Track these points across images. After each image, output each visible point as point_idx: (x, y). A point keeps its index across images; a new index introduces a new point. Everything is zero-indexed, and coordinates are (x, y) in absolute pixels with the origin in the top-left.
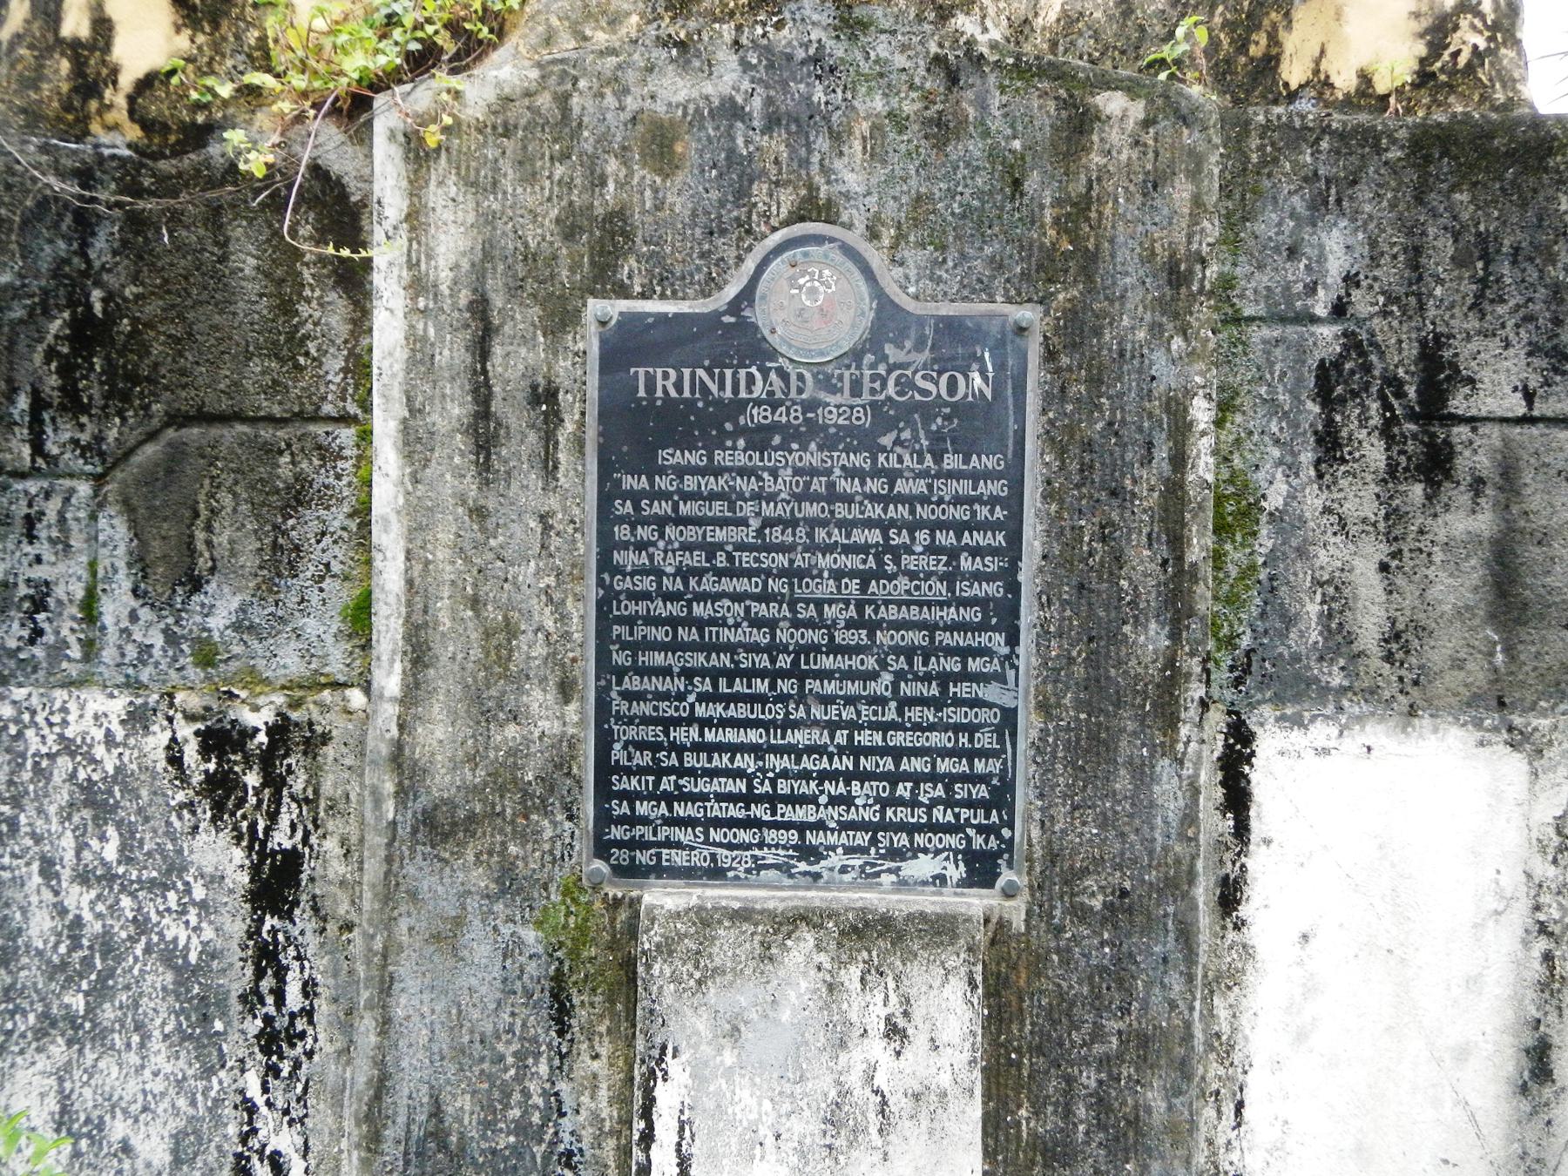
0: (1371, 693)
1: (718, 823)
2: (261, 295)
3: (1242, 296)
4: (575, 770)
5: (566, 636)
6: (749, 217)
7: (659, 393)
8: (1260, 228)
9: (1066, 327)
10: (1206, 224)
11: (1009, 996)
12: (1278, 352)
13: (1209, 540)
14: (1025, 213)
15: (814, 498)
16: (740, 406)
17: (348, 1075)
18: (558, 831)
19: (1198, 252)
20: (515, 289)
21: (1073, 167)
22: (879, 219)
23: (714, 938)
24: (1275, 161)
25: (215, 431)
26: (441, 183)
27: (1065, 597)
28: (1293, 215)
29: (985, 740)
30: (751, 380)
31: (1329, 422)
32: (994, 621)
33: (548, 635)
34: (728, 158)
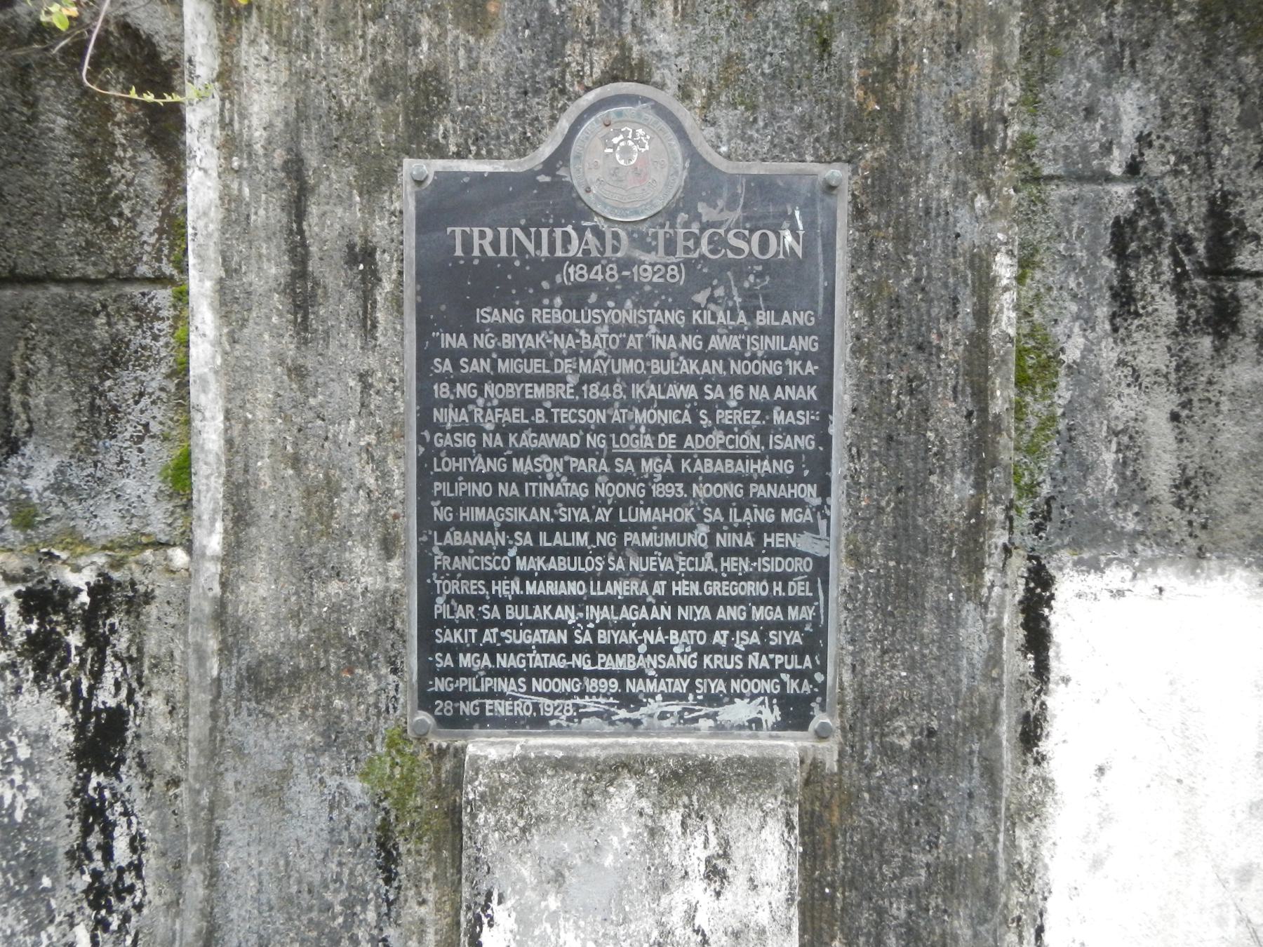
0: (1163, 537)
1: (540, 673)
2: (72, 156)
3: (1041, 156)
4: (398, 625)
5: (388, 493)
6: (563, 77)
7: (476, 253)
8: (1058, 89)
9: (873, 186)
10: (1007, 84)
11: (823, 833)
12: (1076, 210)
13: (1012, 393)
14: (833, 73)
16: (556, 265)
17: (177, 926)
18: (383, 685)
19: (1000, 112)
20: (329, 149)
21: (879, 29)
22: (691, 79)
23: (537, 787)
24: (1073, 23)
25: (29, 293)
26: (253, 42)
27: (875, 448)
28: (1090, 76)
29: (798, 588)
30: (567, 238)
31: (1124, 278)
32: (806, 473)
33: (369, 493)
34: (541, 18)
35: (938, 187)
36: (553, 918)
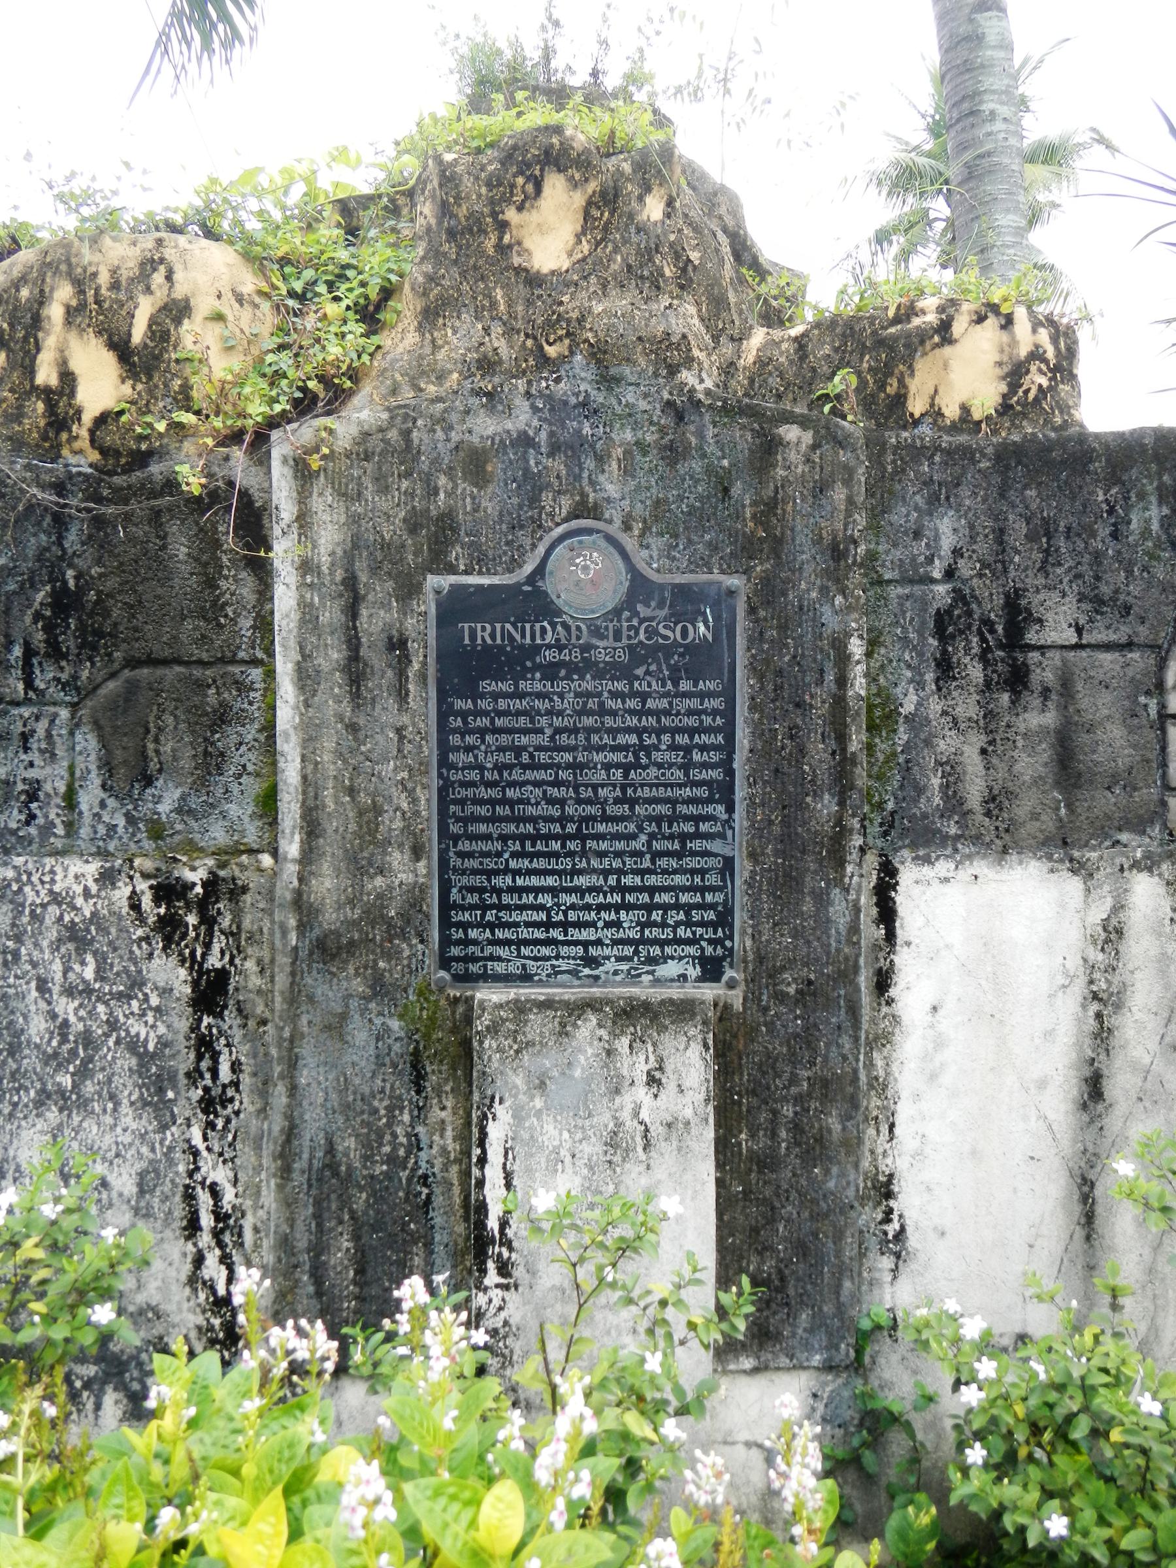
0: (977, 839)
1: (526, 942)
2: (192, 574)
3: (883, 566)
5: (417, 813)
7: (479, 641)
8: (894, 518)
10: (857, 516)
11: (732, 1056)
12: (908, 604)
13: (864, 737)
15: (590, 713)
16: (536, 649)
17: (265, 1127)
19: (852, 536)
20: (375, 570)
23: (526, 1021)
24: (903, 471)
25: (160, 671)
26: (320, 494)
28: (917, 508)
29: (713, 879)
30: (544, 631)
31: (944, 652)
33: (404, 813)
34: (524, 475)
35: (808, 590)
36: (538, 1114)
